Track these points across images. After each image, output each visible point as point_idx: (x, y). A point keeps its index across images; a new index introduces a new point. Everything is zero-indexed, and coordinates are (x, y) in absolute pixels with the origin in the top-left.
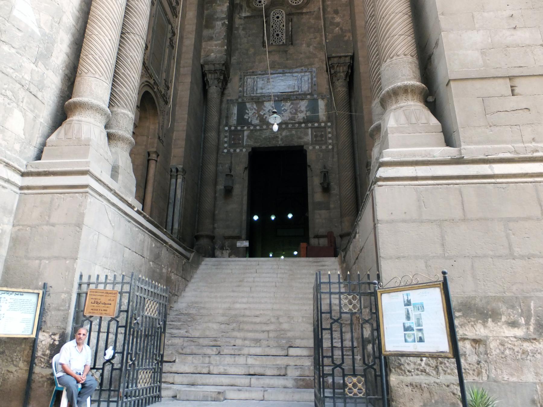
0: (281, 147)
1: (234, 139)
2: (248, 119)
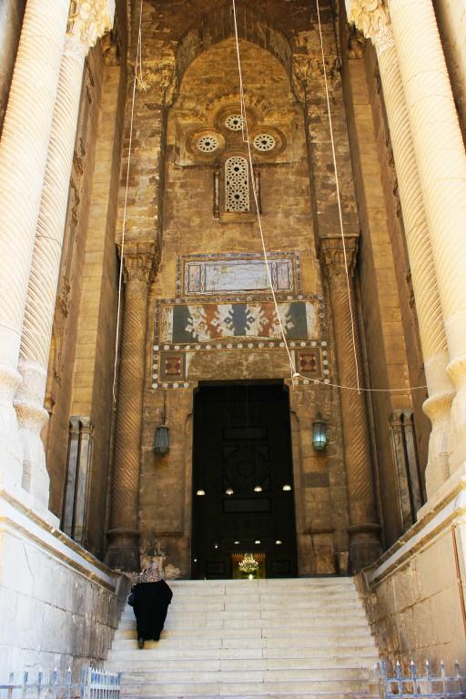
0: (245, 380)
1: (168, 366)
2: (192, 333)
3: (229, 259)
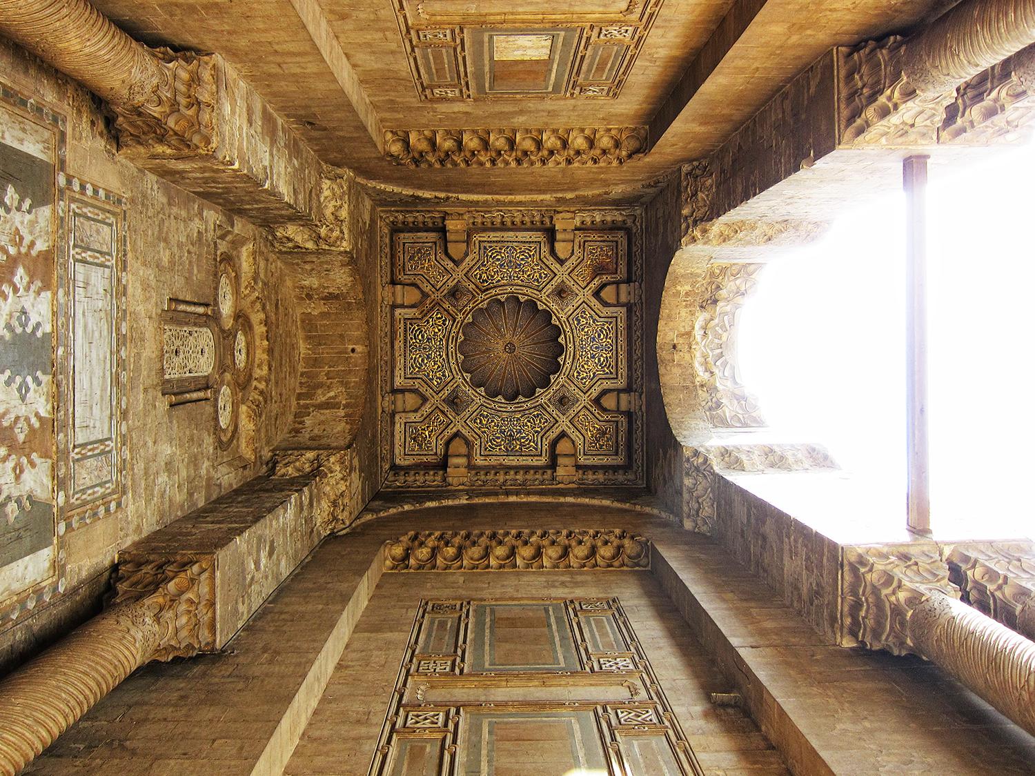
3: (118, 329)
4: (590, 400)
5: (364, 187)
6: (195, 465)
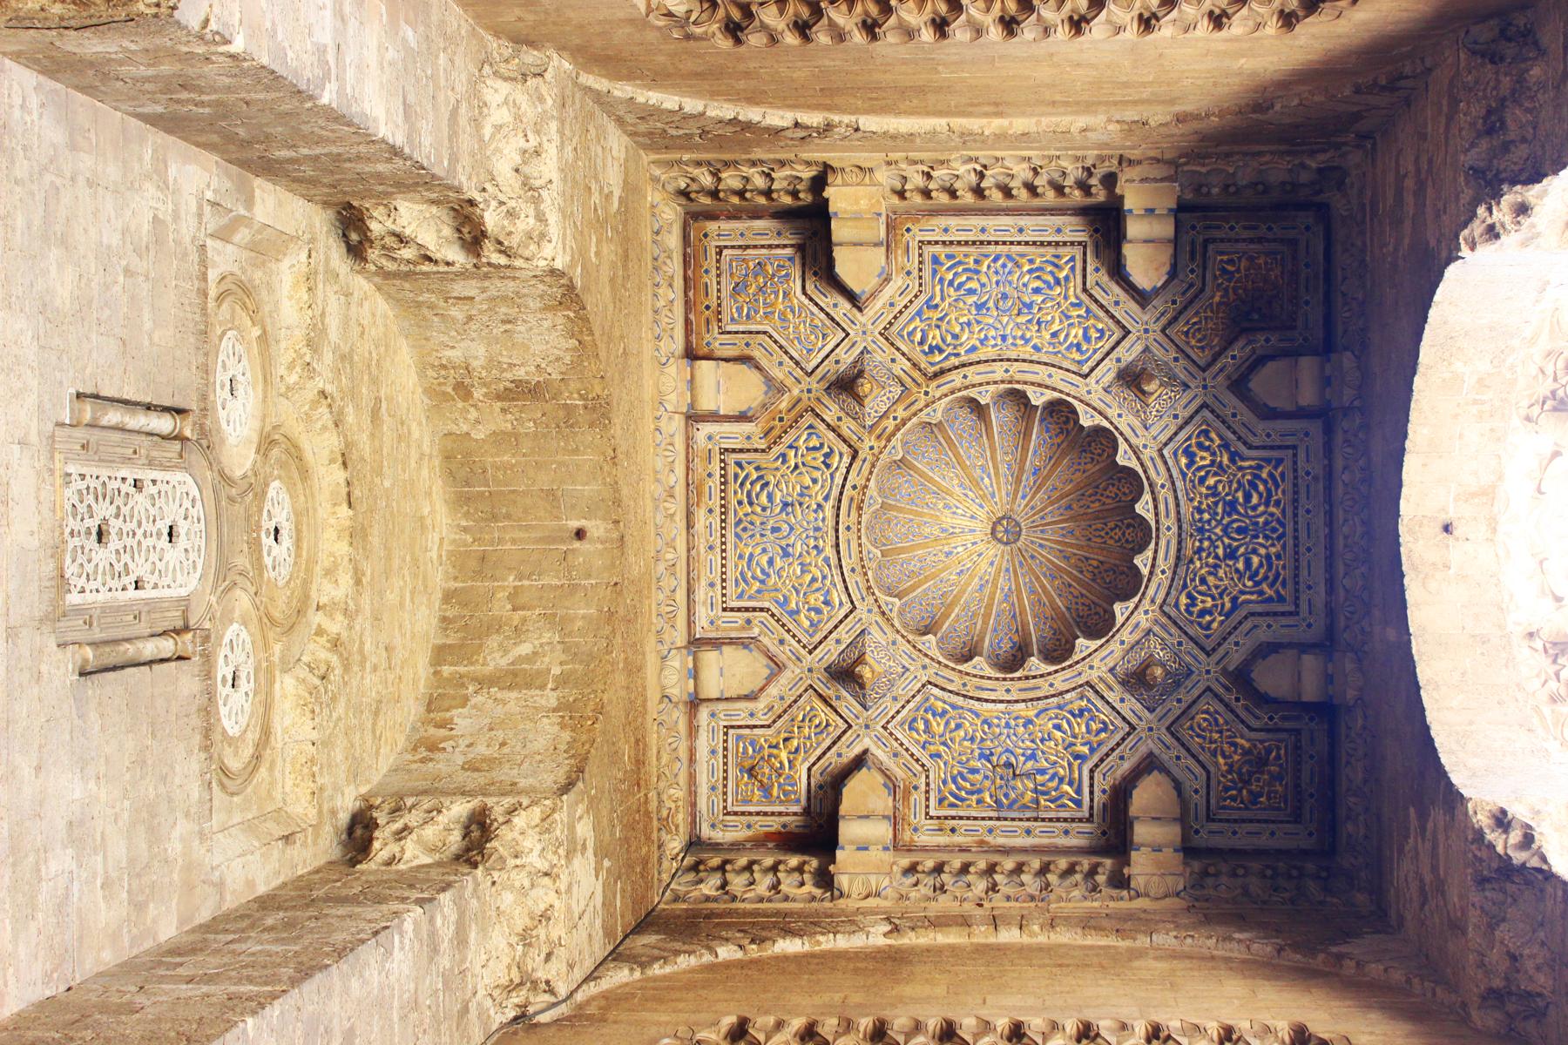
4: (1224, 672)
5: (600, 99)
6: (152, 830)
